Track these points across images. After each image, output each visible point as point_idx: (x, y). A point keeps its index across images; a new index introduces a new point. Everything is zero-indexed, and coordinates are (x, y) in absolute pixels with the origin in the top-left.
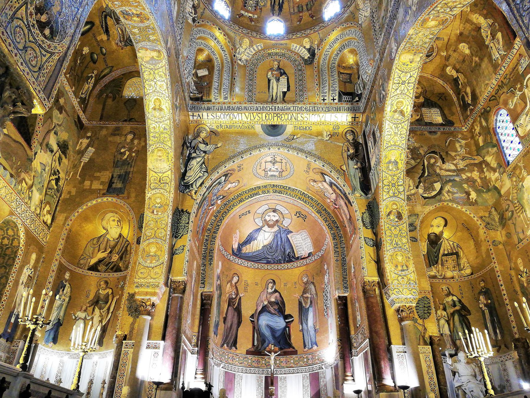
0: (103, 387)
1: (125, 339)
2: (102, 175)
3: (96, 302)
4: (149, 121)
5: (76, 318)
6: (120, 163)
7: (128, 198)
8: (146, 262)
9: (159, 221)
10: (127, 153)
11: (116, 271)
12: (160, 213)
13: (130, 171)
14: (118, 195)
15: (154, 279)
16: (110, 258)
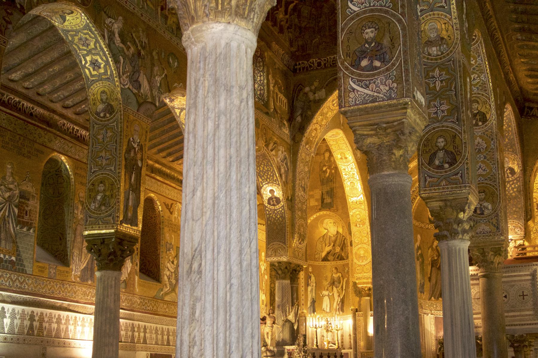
0: (350, 338)
1: (357, 311)
2: (315, 193)
3: (333, 283)
4: (340, 166)
5: (323, 295)
6: (325, 181)
7: (337, 211)
8: (359, 261)
9: (362, 231)
10: (328, 171)
11: (341, 260)
12: (361, 226)
13: (333, 188)
14: (329, 209)
15: (367, 273)
16: (334, 249)
